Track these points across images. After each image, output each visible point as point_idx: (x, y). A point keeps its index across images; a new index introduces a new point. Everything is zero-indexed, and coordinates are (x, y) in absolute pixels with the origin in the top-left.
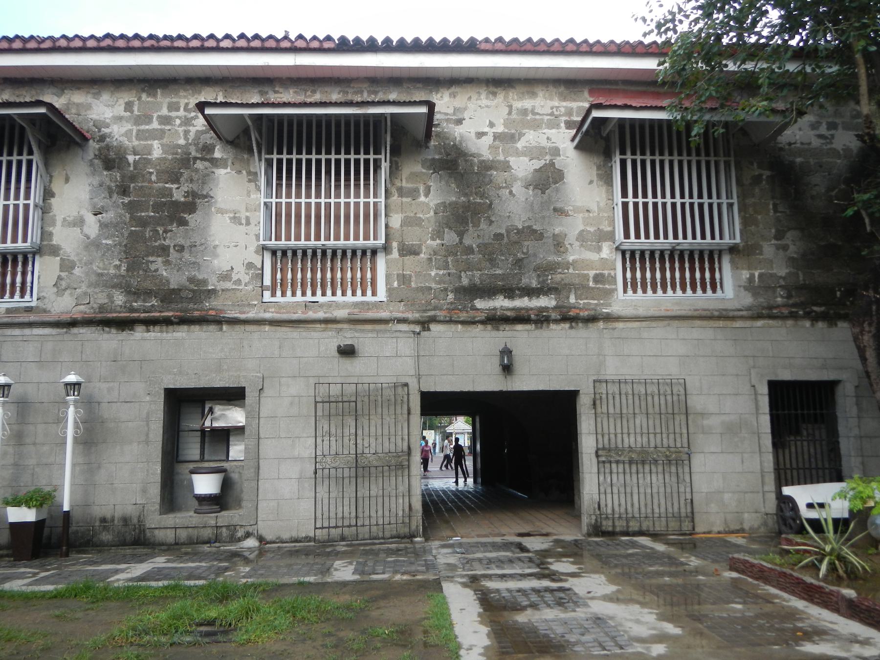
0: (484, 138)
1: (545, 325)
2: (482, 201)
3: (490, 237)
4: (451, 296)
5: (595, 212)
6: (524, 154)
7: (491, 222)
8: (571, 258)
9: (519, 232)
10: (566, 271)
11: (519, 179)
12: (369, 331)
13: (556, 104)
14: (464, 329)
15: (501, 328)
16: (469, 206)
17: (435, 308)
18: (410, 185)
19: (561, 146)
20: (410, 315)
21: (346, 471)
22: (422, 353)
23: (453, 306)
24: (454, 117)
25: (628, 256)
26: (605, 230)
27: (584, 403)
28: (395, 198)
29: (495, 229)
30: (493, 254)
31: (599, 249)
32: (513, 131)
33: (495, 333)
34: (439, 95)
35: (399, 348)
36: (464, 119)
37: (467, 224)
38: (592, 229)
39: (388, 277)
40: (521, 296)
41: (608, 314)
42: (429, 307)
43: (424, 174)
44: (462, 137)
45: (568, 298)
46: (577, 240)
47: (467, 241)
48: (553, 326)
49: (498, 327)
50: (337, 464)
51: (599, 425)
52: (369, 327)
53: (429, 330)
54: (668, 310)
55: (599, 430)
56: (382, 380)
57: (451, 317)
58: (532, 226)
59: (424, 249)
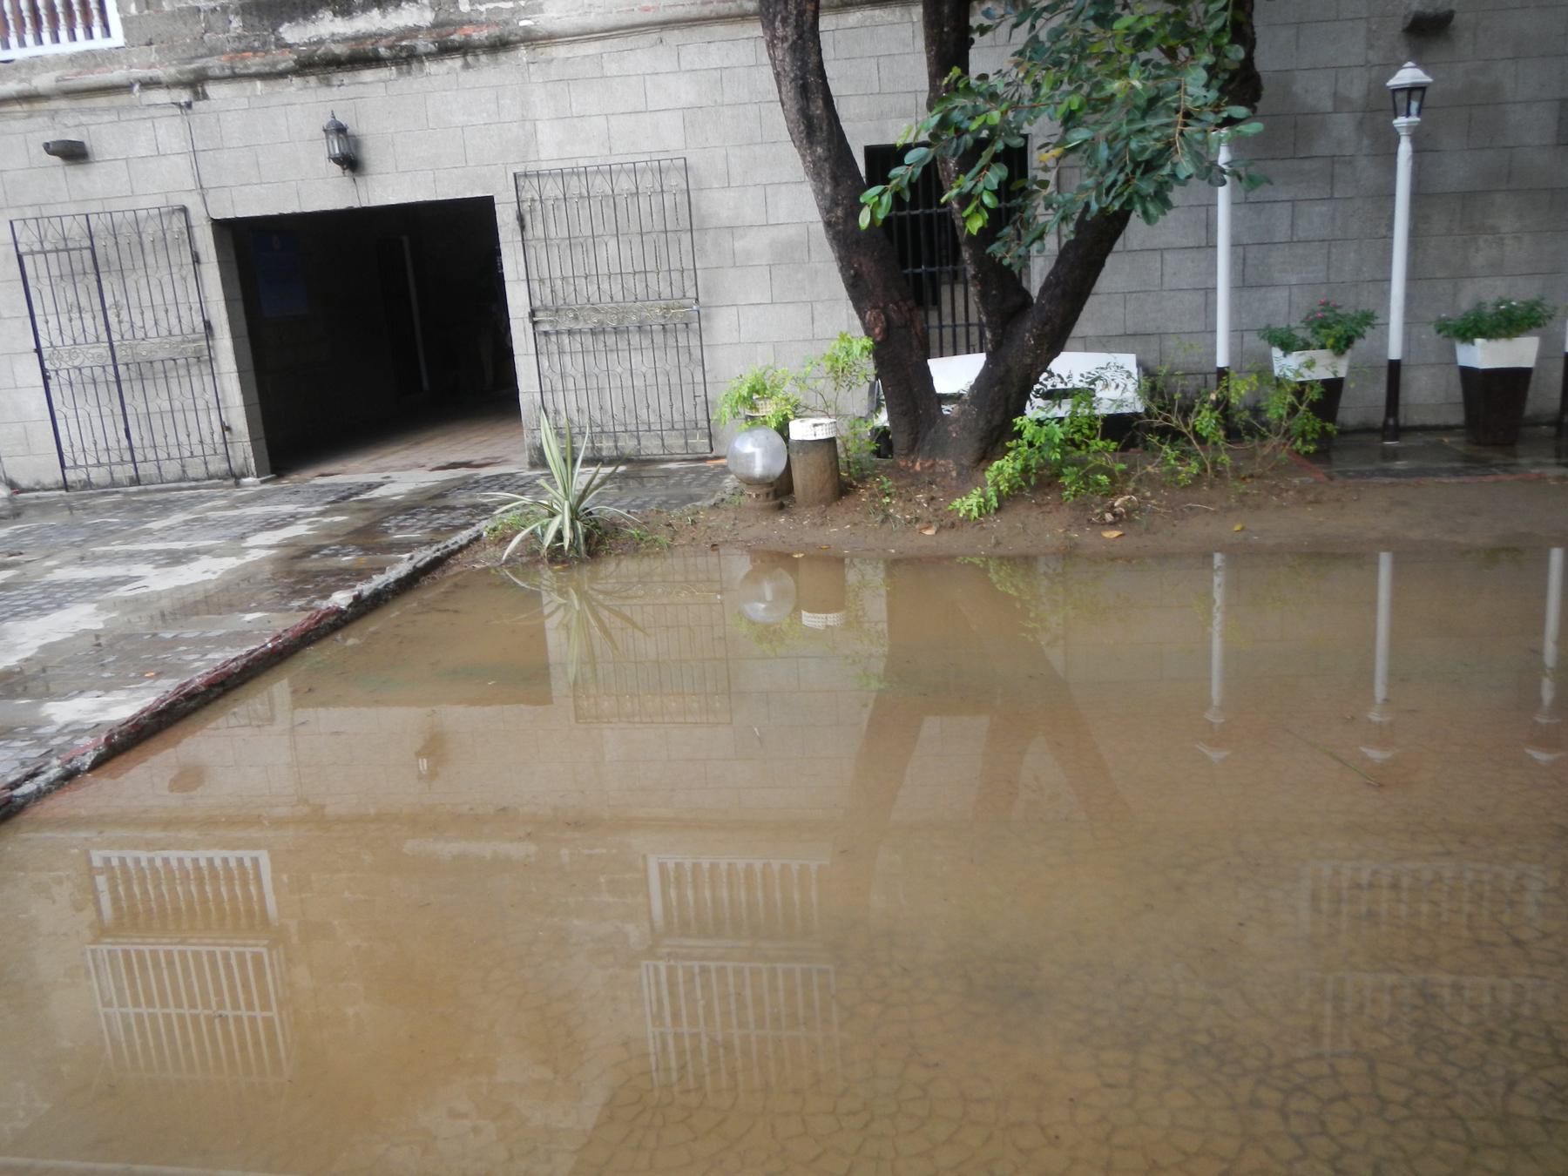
1: (415, 65)
4: (236, 23)
12: (107, 110)
15: (335, 81)
17: (212, 52)
20: (159, 73)
21: (98, 372)
22: (199, 146)
27: (505, 218)
33: (325, 93)
35: (159, 139)
41: (527, 30)
42: (202, 51)
48: (431, 67)
49: (327, 79)
50: (77, 363)
51: (533, 265)
52: (102, 101)
53: (205, 97)
54: (646, 9)
55: (534, 275)
56: (144, 202)
57: (232, 68)
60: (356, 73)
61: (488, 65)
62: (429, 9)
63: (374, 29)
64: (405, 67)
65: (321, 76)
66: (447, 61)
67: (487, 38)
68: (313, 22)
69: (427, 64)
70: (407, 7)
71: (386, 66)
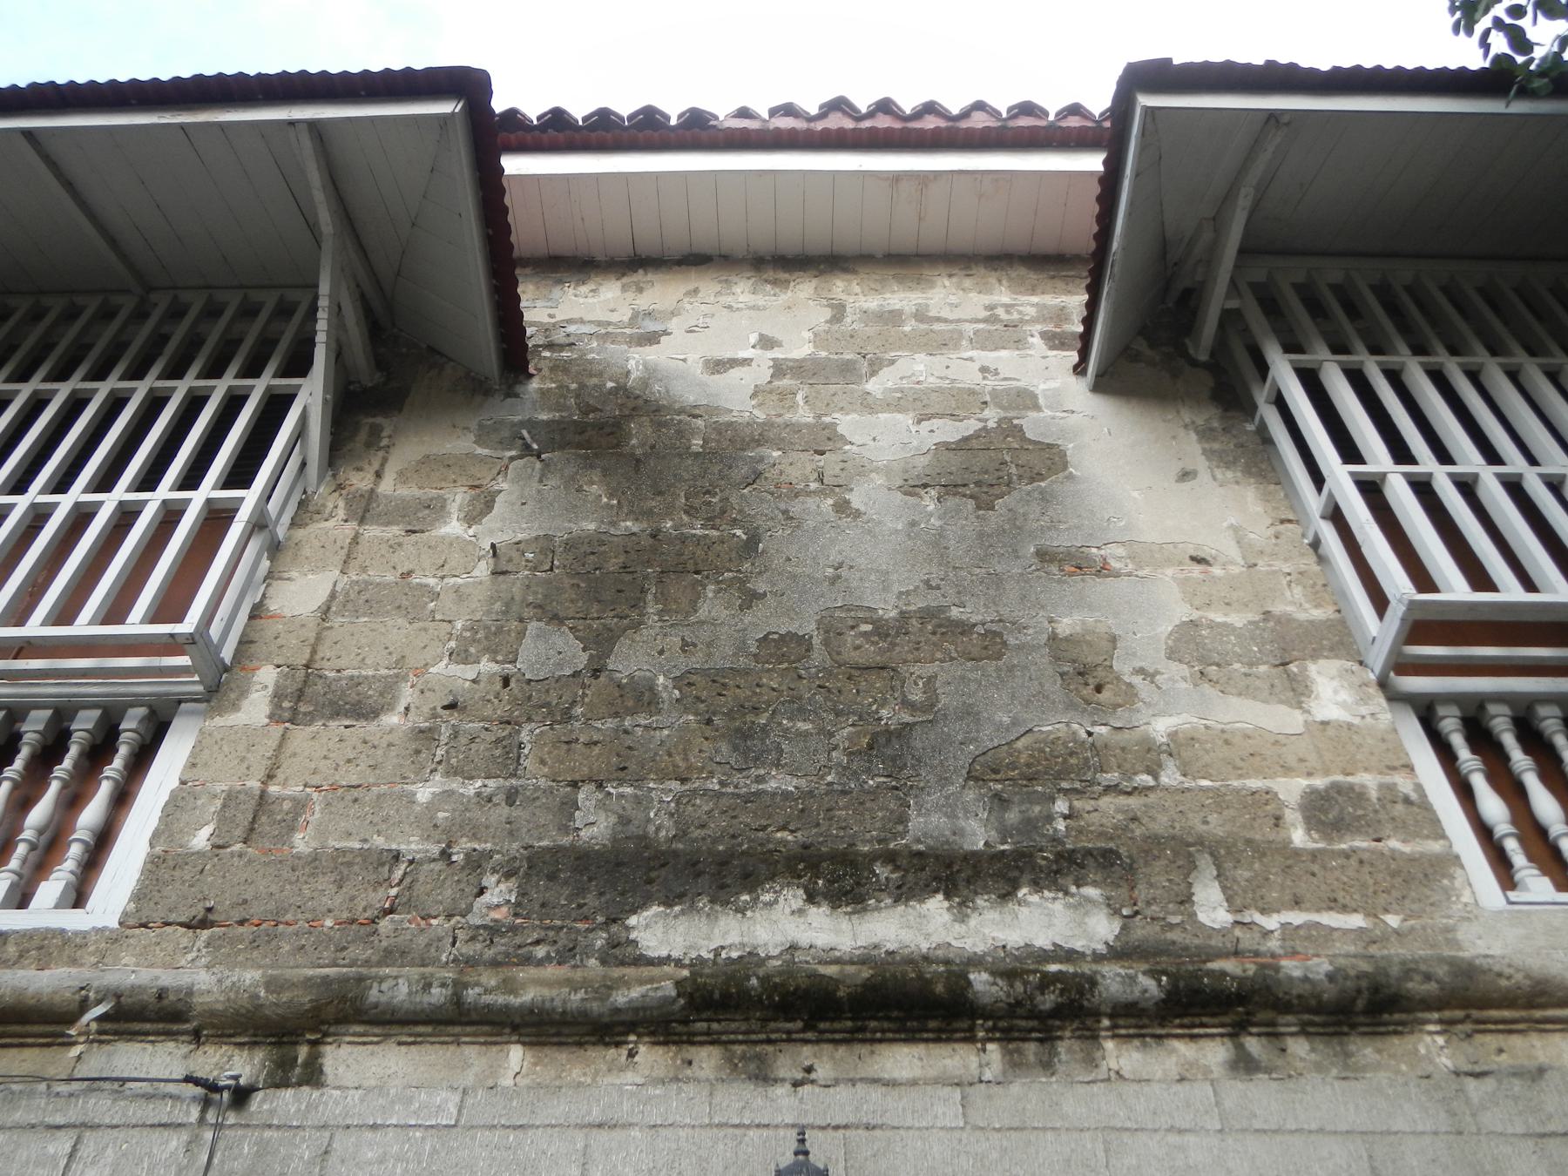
0: (735, 373)
2: (715, 533)
3: (741, 647)
4: (498, 893)
5: (1232, 563)
6: (896, 403)
7: (751, 598)
8: (1160, 727)
9: (881, 630)
10: (1145, 779)
11: (876, 470)
13: (1006, 299)
14: (545, 1073)
15: (786, 1063)
16: (654, 550)
18: (408, 492)
19: (1041, 387)
23: (502, 945)
24: (628, 331)
25: (1451, 725)
26: (1302, 616)
28: (331, 524)
29: (766, 620)
30: (756, 710)
31: (1297, 692)
32: (848, 356)
33: (741, 1100)
34: (584, 289)
36: (666, 333)
37: (637, 604)
38: (1238, 619)
39: (175, 806)
40: (904, 893)
43: (482, 460)
44: (651, 372)
45: (1186, 900)
46: (1172, 654)
47: (628, 661)
48: (1119, 1055)
49: (760, 1058)
53: (313, 1076)
58: (942, 609)
59: (407, 695)
60: (864, 1049)
61: (1319, 1068)
62: (1106, 910)
63: (924, 946)
64: (1031, 1048)
65: (738, 1049)
66: (1177, 1044)
67: (1331, 977)
68: (741, 910)
69: (1109, 1045)
70: (1035, 898)
71: (970, 1039)
